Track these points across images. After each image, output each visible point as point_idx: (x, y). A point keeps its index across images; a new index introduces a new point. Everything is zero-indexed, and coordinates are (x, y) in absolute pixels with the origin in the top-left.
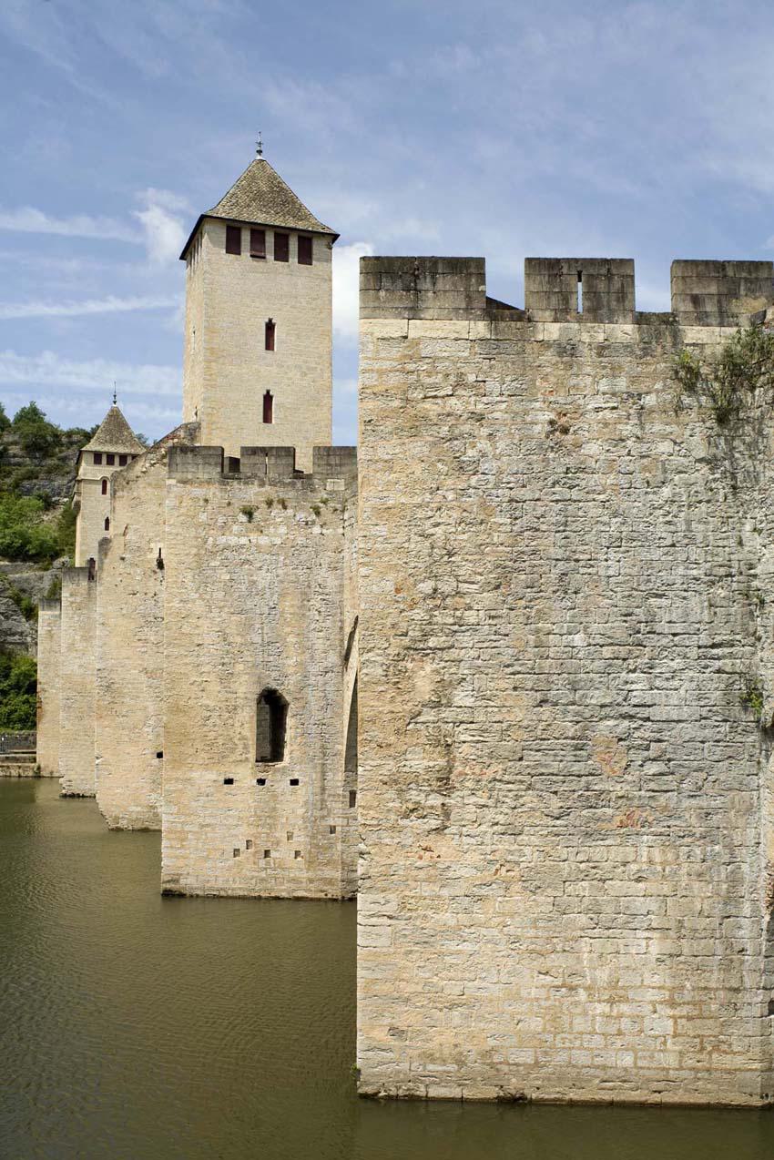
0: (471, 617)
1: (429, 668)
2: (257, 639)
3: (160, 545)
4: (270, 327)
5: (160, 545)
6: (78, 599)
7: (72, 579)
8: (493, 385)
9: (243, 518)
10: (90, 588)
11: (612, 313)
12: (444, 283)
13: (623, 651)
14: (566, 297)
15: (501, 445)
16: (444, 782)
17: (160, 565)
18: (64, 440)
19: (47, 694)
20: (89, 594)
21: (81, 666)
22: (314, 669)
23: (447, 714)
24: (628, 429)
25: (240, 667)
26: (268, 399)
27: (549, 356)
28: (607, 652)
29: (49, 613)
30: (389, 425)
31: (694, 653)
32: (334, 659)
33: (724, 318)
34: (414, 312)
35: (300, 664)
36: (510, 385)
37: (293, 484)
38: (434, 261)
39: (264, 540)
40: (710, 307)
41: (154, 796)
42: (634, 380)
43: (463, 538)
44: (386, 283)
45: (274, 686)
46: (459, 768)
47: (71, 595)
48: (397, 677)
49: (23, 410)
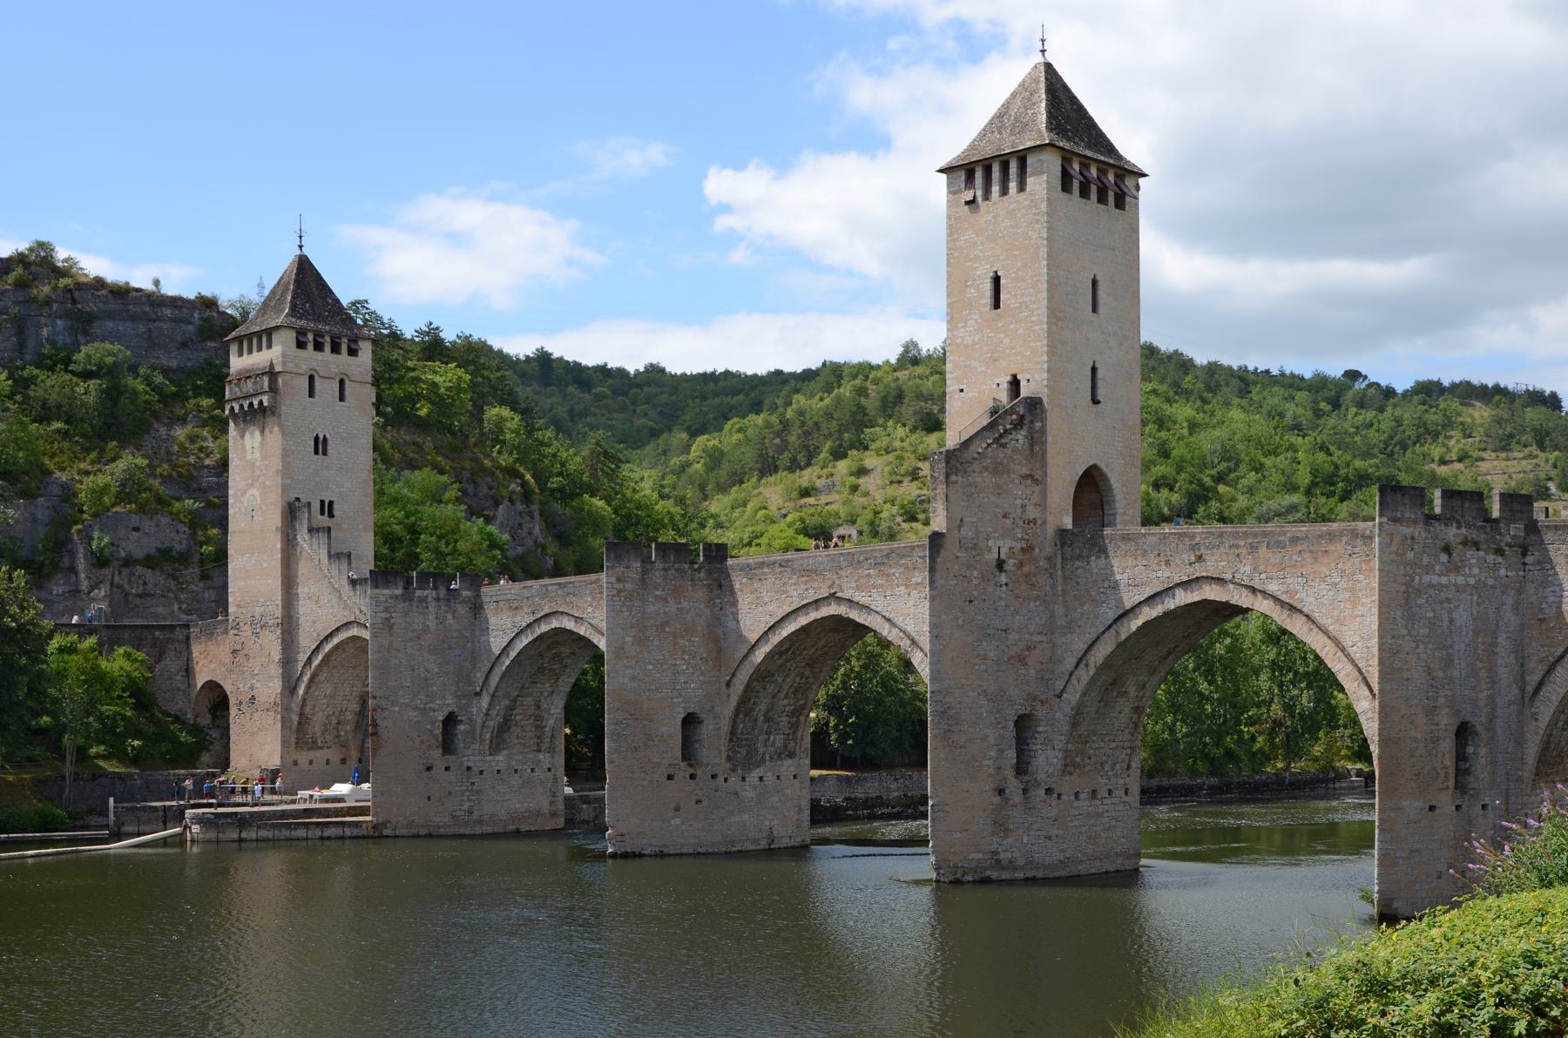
2: (1456, 674)
3: (999, 543)
5: (999, 543)
6: (629, 586)
7: (619, 558)
9: (1444, 558)
10: (644, 572)
17: (1000, 565)
19: (386, 714)
20: (643, 580)
21: (634, 678)
22: (1500, 702)
25: (1441, 700)
29: (386, 592)
32: (1515, 691)
35: (1491, 699)
37: (1483, 527)
39: (1461, 580)
41: (995, 839)
45: (1468, 718)
47: (619, 580)
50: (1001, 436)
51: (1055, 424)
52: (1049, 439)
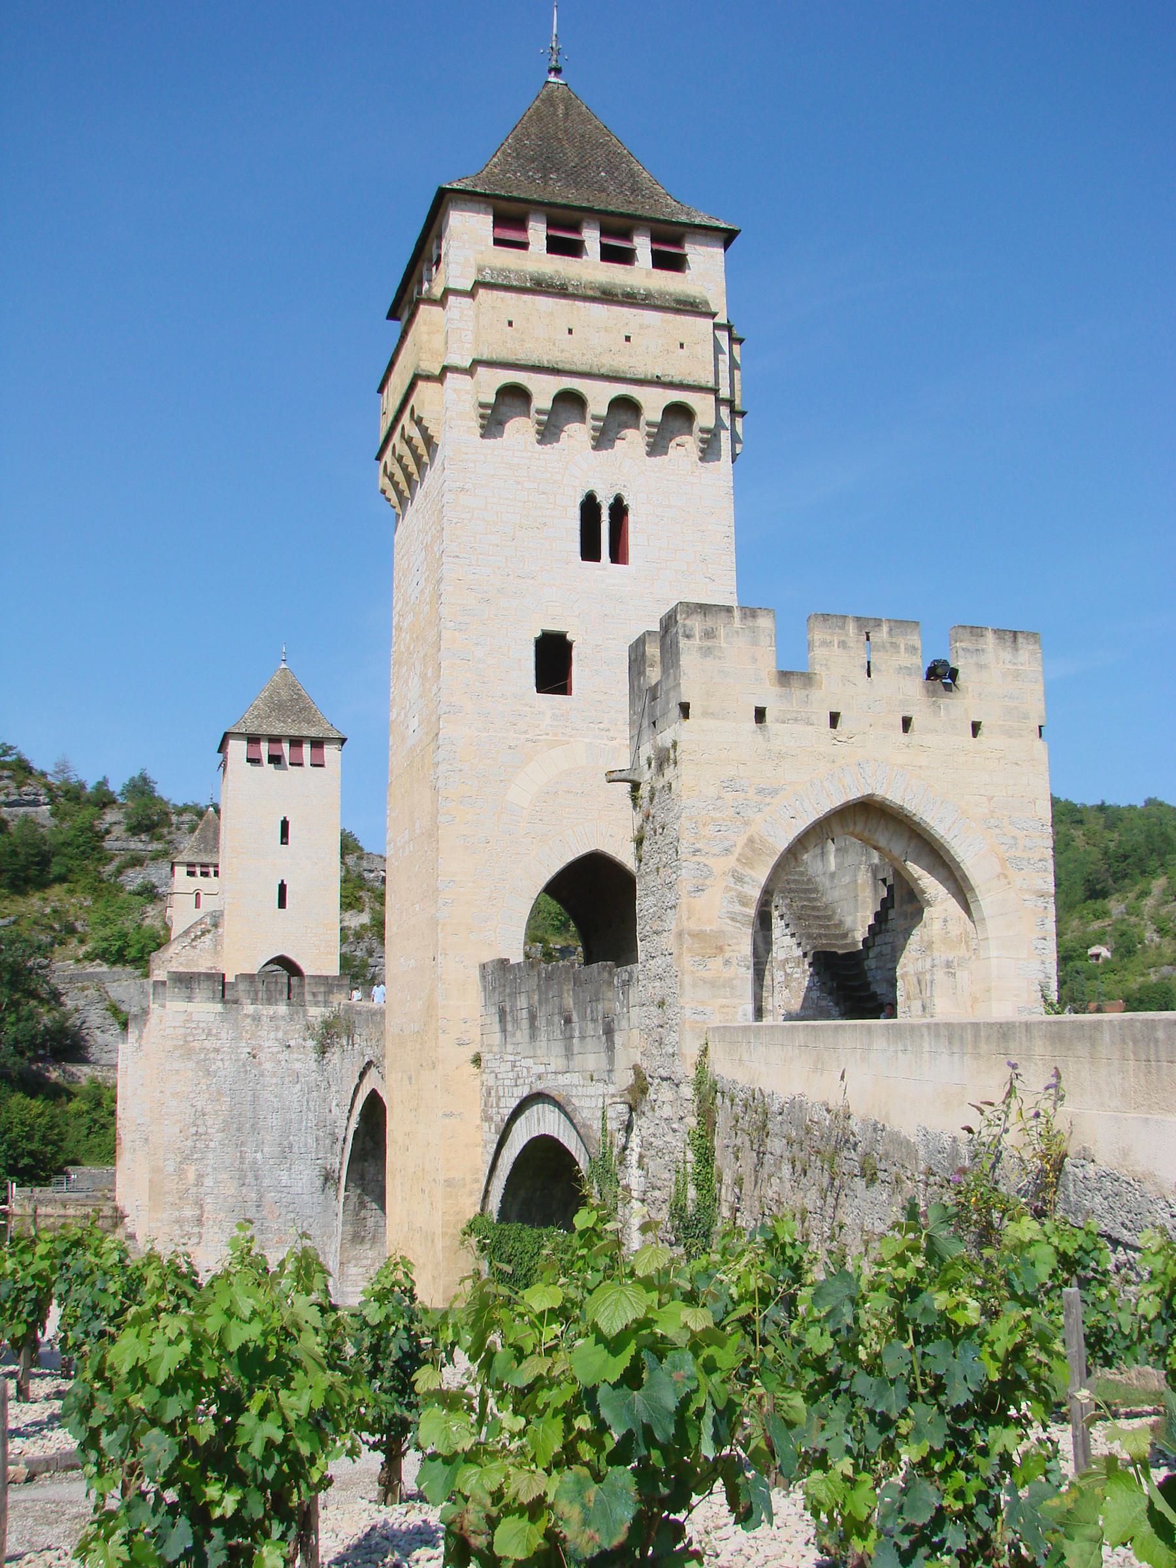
0: (212, 1144)
1: (193, 1168)
4: (285, 825)
8: (224, 1035)
11: (277, 1001)
12: (204, 985)
13: (278, 1161)
14: (257, 994)
15: (227, 1063)
16: (199, 1221)
18: (174, 818)
23: (202, 1190)
24: (281, 1057)
26: (282, 888)
27: (249, 1020)
28: (271, 1162)
30: (178, 1053)
31: (309, 1162)
33: (326, 1003)
34: (190, 999)
36: (232, 1034)
38: (200, 974)
40: (321, 998)
42: (285, 1033)
43: (209, 1109)
44: (178, 984)
46: (206, 1215)
48: (180, 1172)
49: (132, 779)
50: (193, 940)
51: (228, 927)
52: (226, 941)
